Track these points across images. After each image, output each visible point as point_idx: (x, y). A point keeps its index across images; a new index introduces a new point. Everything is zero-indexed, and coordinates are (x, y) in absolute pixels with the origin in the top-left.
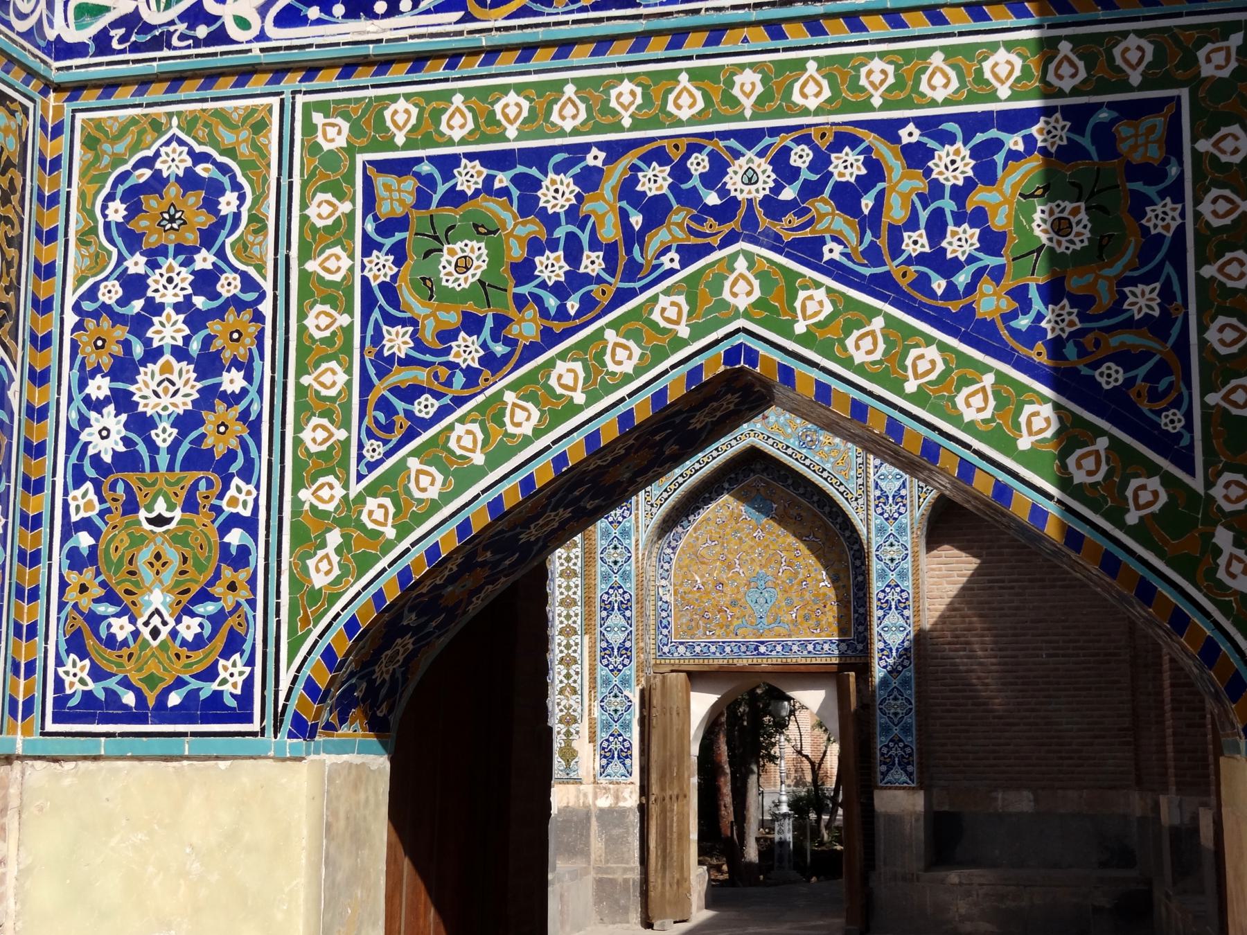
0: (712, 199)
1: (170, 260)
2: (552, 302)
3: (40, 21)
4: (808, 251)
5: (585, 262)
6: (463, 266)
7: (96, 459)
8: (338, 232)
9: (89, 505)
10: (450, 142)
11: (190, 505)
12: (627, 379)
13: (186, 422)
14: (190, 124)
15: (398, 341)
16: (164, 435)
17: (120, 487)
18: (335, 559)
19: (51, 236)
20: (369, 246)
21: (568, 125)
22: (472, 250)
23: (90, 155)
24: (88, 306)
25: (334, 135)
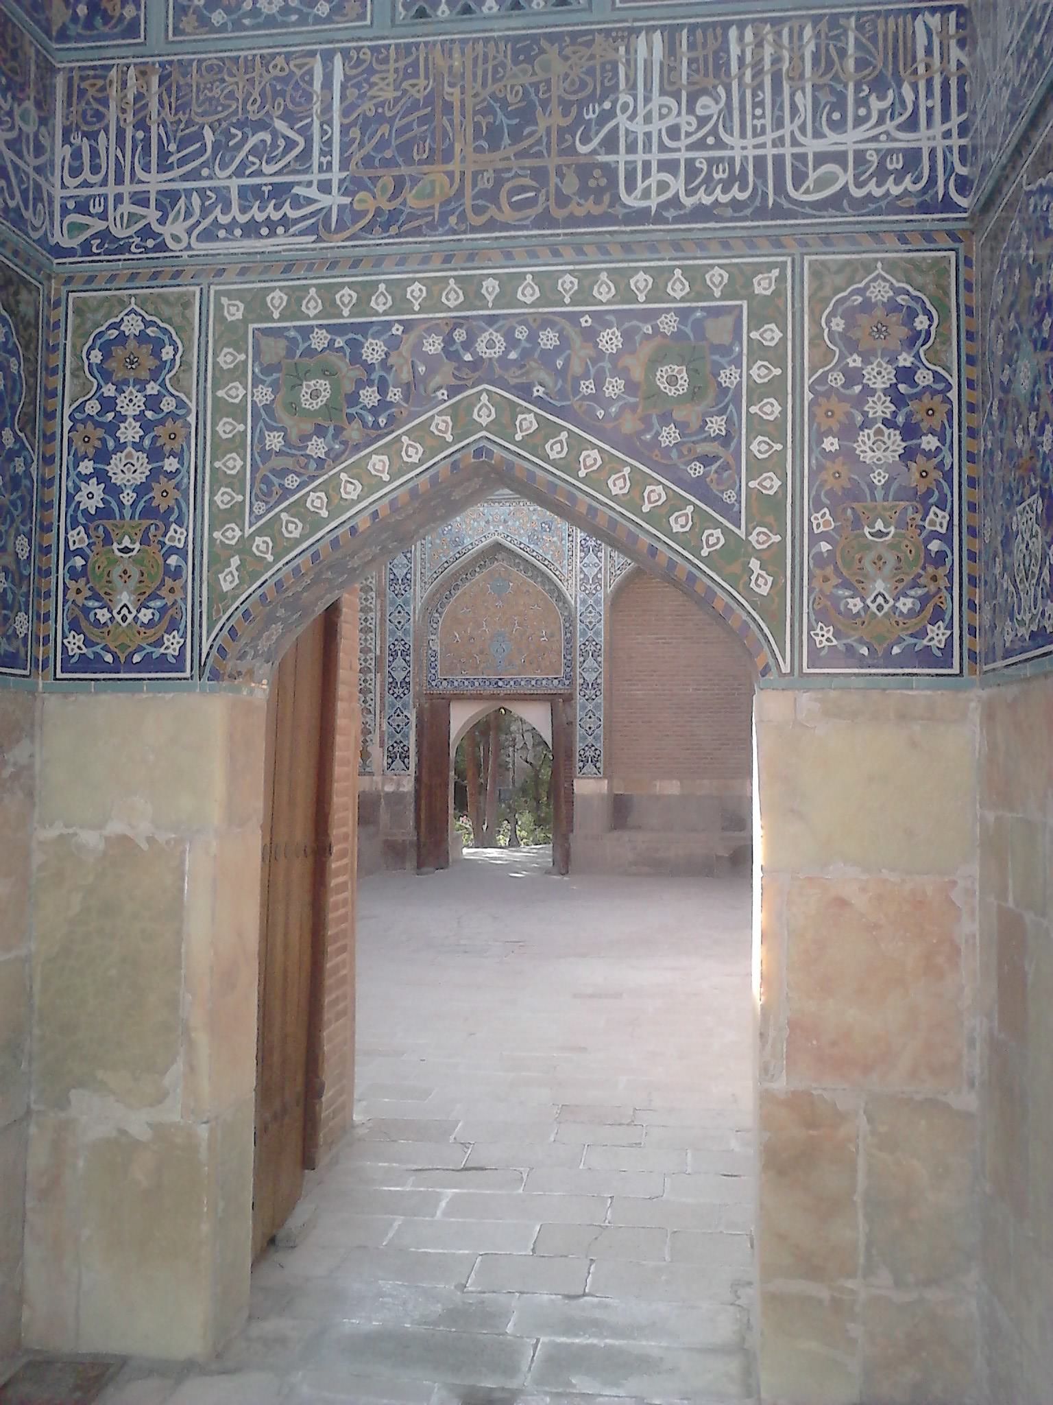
0: (468, 357)
1: (131, 388)
2: (370, 419)
3: (45, 234)
4: (524, 391)
5: (390, 394)
6: (315, 395)
7: (85, 511)
8: (238, 372)
9: (81, 541)
10: (308, 318)
11: (145, 541)
12: (415, 466)
13: (141, 489)
14: (142, 302)
15: (274, 441)
16: (128, 498)
17: (101, 528)
18: (236, 574)
19: (54, 372)
21: (381, 309)
22: (321, 385)
23: (79, 320)
24: (78, 416)
25: (235, 312)
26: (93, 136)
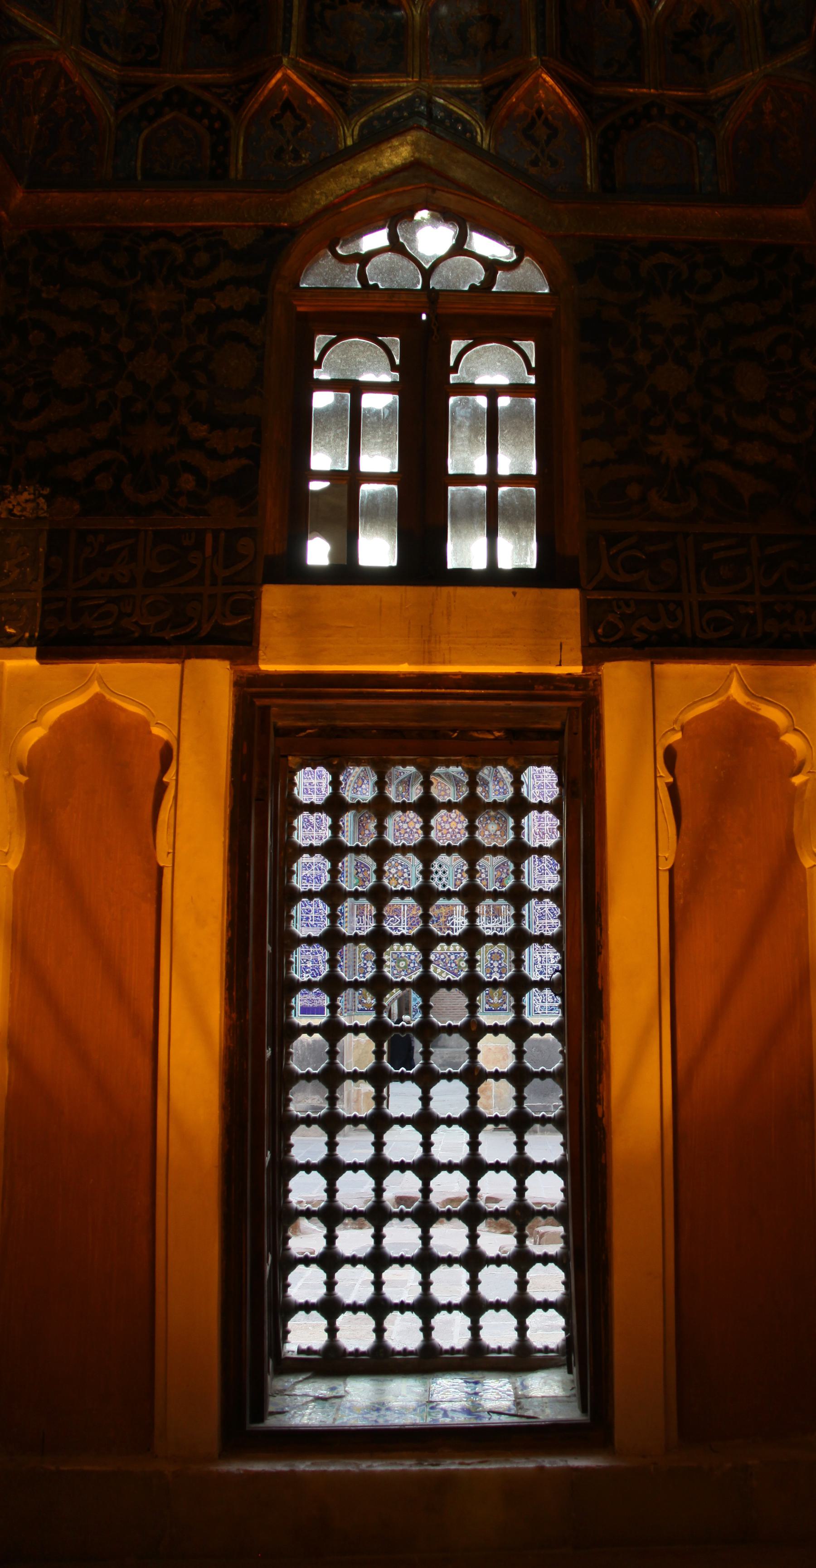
4: (438, 965)
20: (392, 961)
26: (362, 916)
